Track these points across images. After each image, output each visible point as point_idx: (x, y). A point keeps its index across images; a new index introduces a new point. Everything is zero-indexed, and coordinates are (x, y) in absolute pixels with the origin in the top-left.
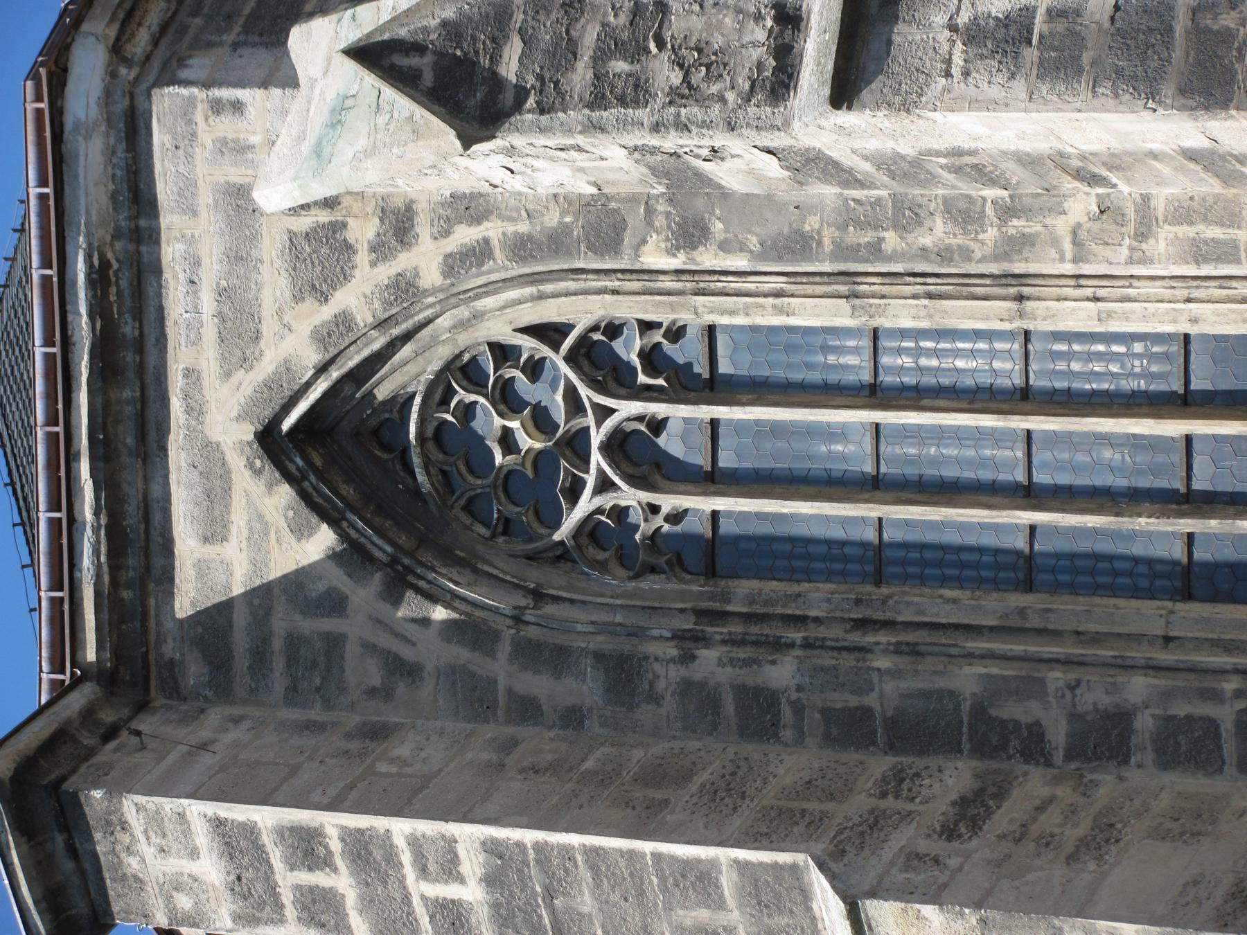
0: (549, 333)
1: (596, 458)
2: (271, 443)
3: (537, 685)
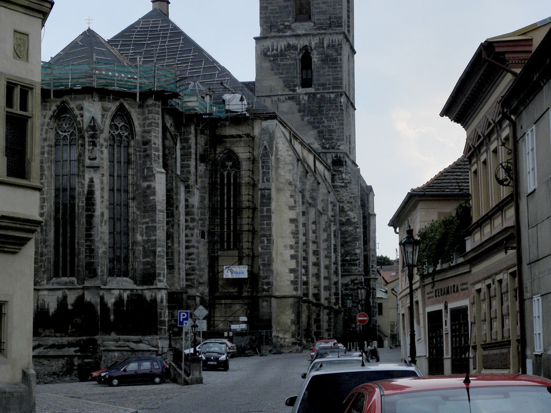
0: (75, 129)
1: (64, 134)
2: (63, 102)
3: (44, 130)
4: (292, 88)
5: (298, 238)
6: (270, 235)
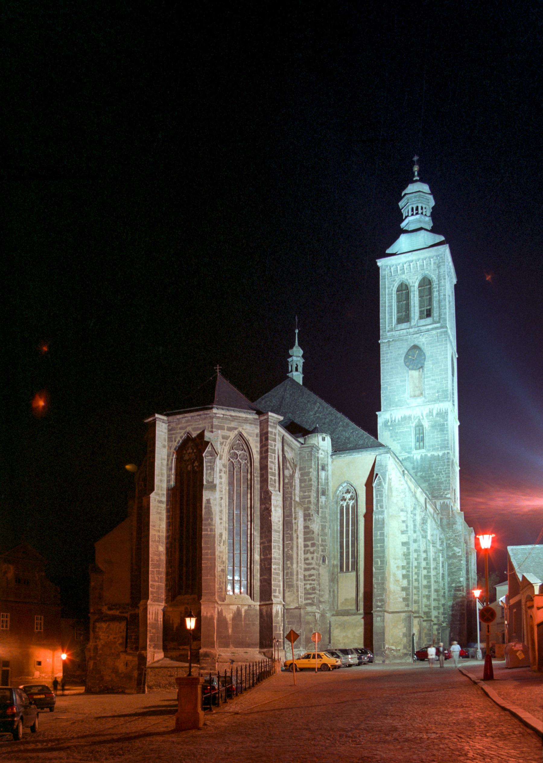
4: (408, 450)
5: (409, 559)
6: (384, 557)
